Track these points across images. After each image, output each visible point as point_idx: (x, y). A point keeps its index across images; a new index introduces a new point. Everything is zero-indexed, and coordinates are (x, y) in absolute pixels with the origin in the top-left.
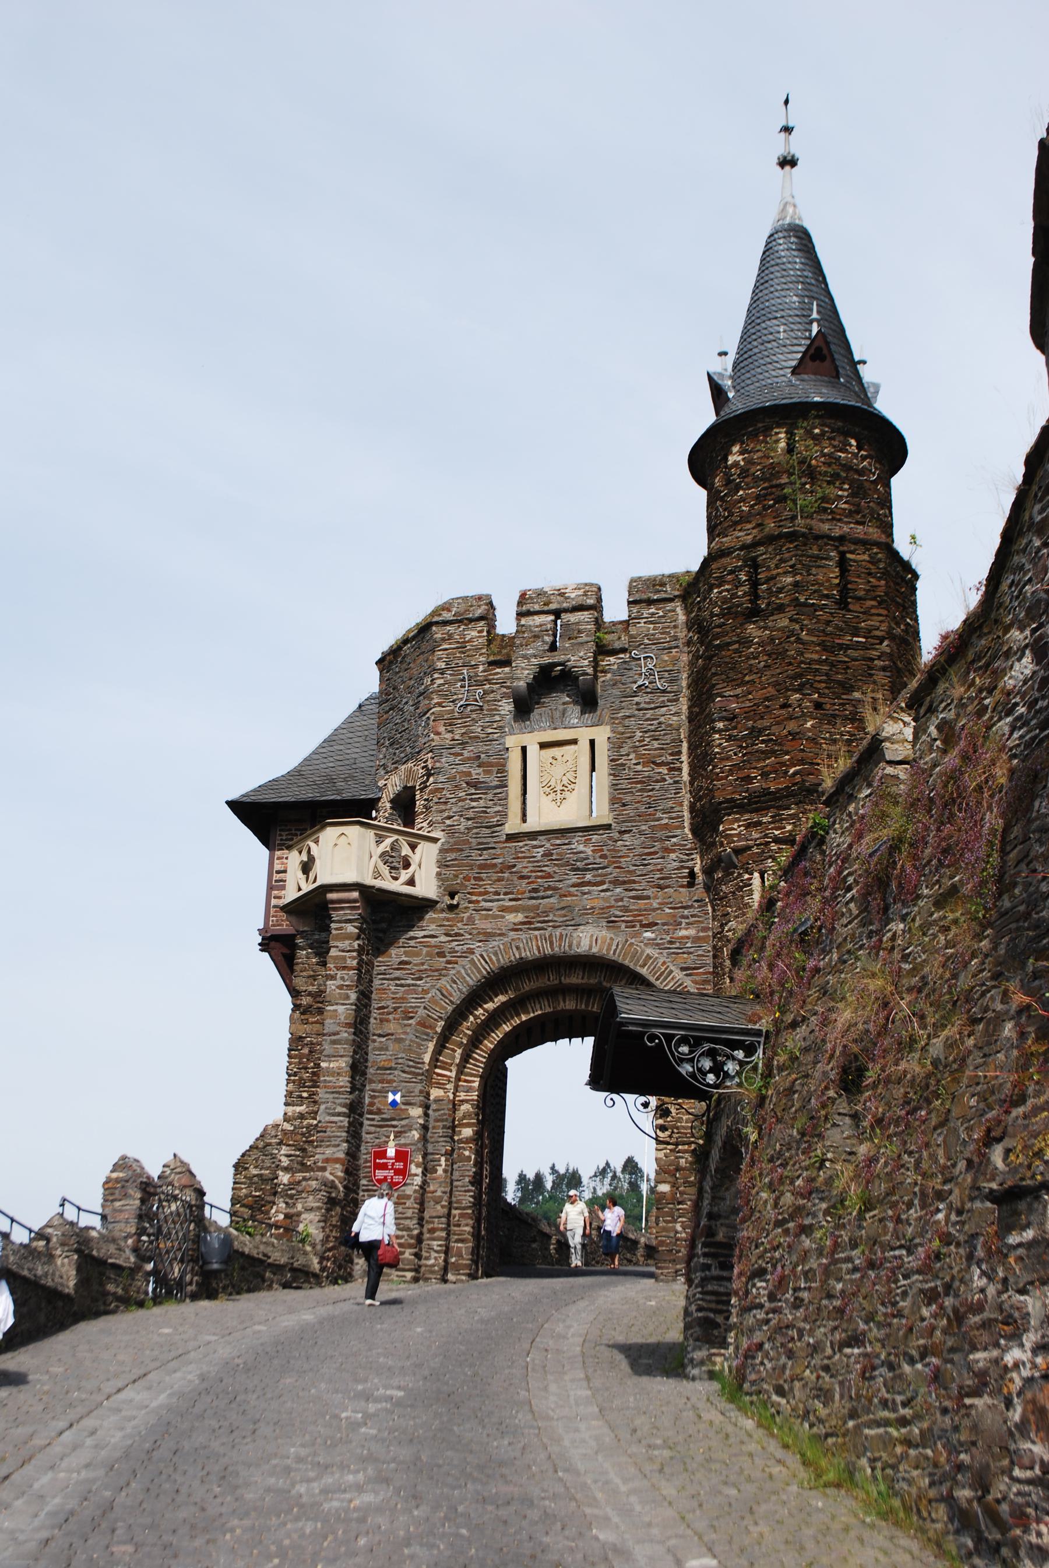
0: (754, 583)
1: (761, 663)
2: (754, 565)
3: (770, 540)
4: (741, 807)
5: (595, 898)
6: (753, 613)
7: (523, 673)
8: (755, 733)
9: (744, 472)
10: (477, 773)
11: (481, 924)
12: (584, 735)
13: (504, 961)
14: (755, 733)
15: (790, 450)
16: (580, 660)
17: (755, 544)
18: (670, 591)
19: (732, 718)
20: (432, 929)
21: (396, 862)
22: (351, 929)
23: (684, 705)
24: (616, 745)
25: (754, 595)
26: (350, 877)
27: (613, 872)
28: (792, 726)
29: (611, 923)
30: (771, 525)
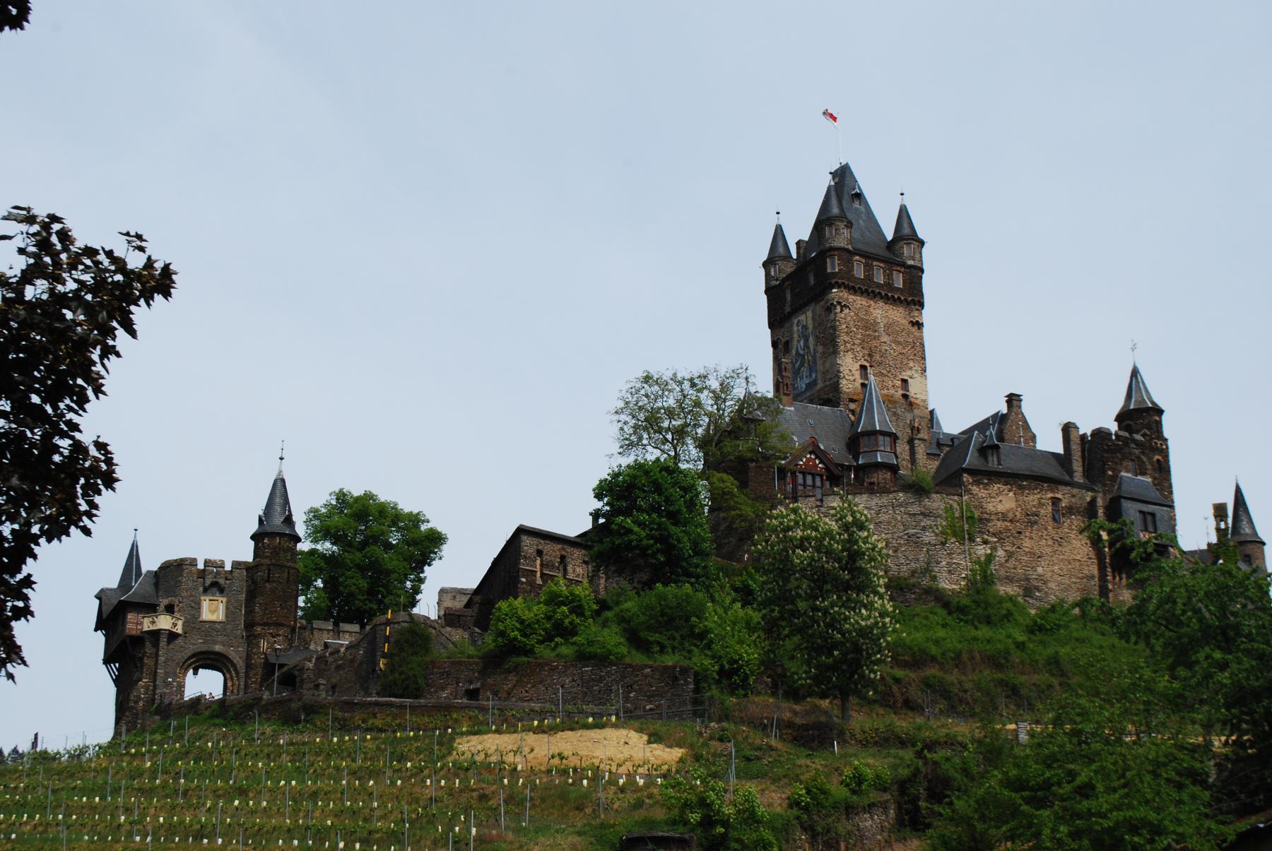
0: (269, 574)
1: (269, 593)
2: (269, 570)
3: (274, 565)
4: (261, 625)
5: (220, 638)
6: (268, 581)
7: (208, 582)
8: (266, 609)
9: (268, 546)
10: (193, 605)
11: (192, 641)
12: (220, 599)
13: (198, 650)
14: (266, 609)
15: (280, 543)
16: (222, 581)
17: (270, 565)
18: (243, 566)
19: (260, 604)
20: (180, 641)
21: (175, 625)
22: (165, 640)
23: (244, 596)
24: (227, 603)
25: (269, 577)
26: (167, 628)
27: (225, 633)
28: (274, 609)
29: (224, 645)
30: (274, 561)
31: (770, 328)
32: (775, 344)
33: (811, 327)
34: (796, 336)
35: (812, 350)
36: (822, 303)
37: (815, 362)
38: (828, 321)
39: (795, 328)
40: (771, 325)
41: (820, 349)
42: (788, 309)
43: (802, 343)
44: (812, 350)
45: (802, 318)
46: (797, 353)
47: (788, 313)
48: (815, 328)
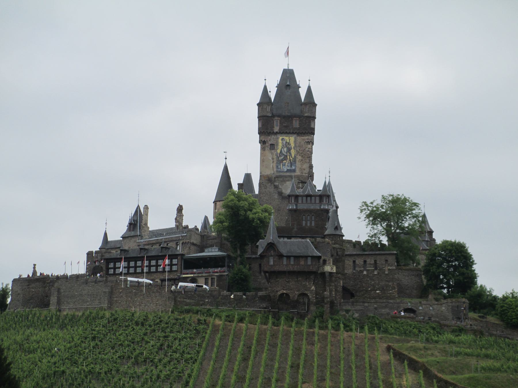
31: (259, 133)
32: (263, 142)
33: (293, 145)
34: (280, 145)
35: (293, 156)
36: (303, 138)
37: (295, 161)
38: (307, 147)
39: (280, 141)
40: (260, 133)
41: (299, 158)
42: (276, 129)
43: (285, 149)
44: (293, 156)
45: (286, 138)
46: (281, 151)
47: (277, 132)
48: (295, 146)
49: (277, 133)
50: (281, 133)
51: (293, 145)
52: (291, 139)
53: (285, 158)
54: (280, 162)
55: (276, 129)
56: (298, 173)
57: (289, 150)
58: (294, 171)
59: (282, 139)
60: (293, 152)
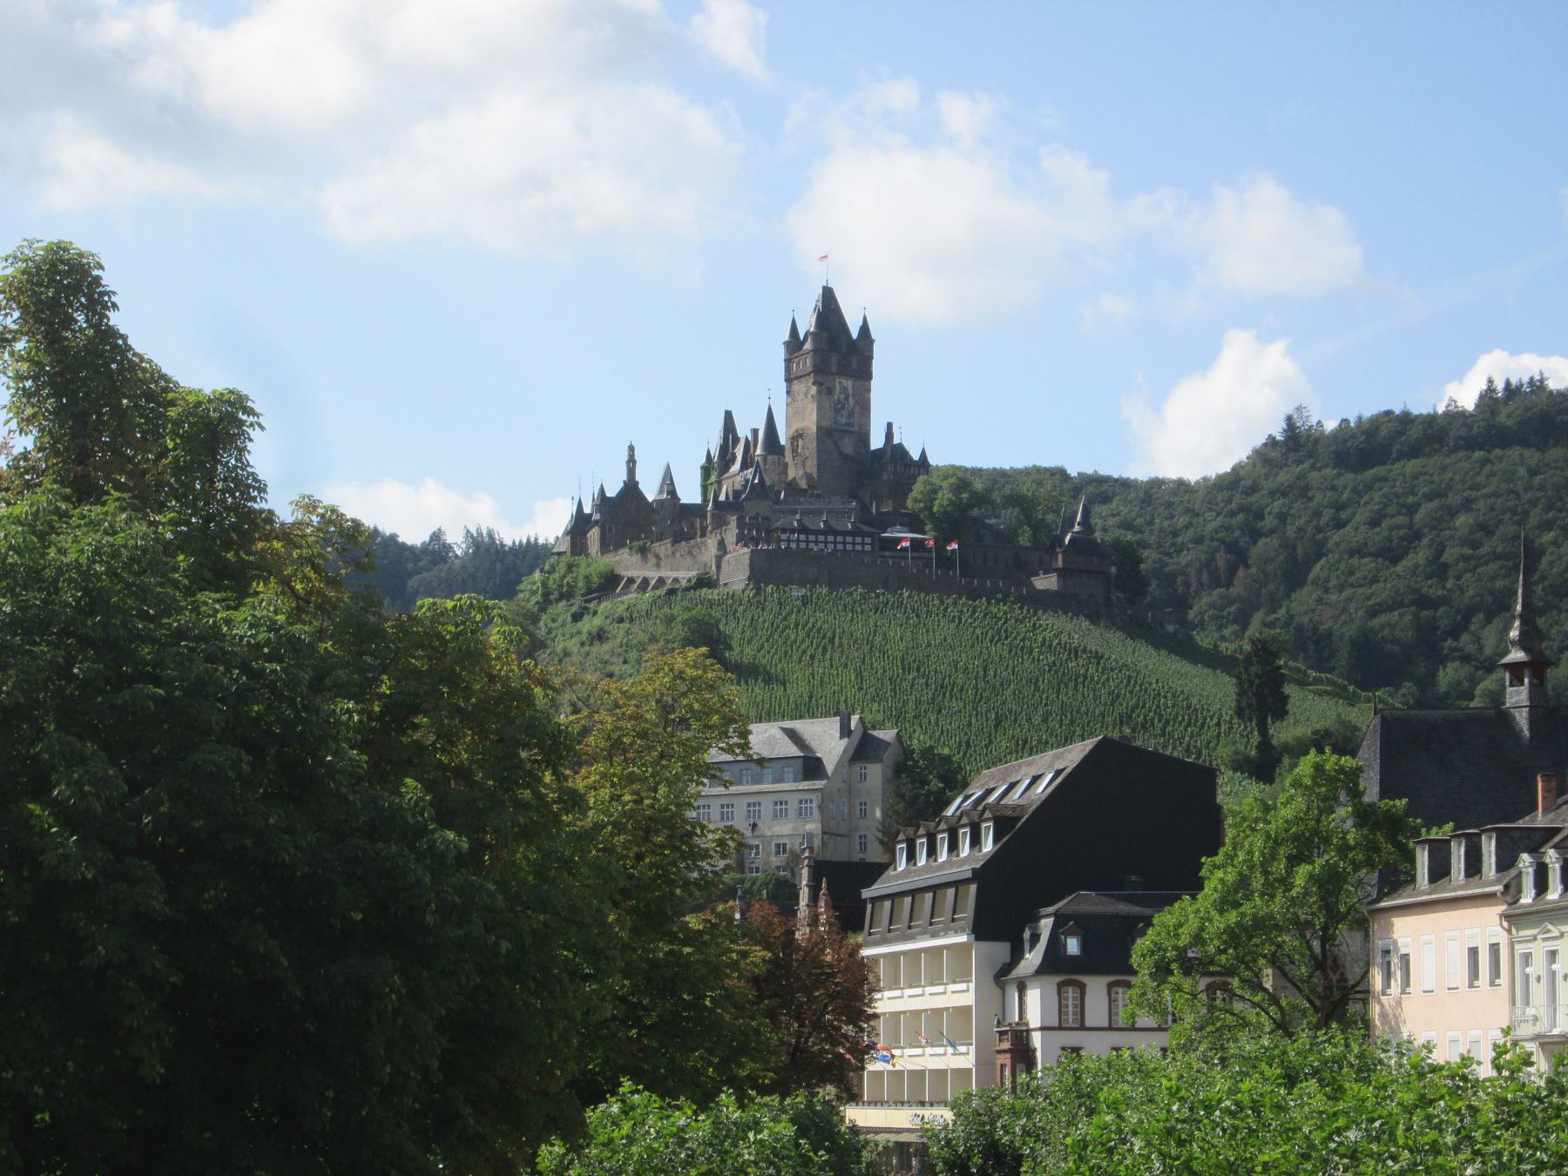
33: (850, 391)
37: (853, 413)
41: (857, 409)
42: (834, 370)
45: (844, 381)
49: (833, 374)
50: (840, 374)
51: (850, 391)
52: (848, 383)
53: (843, 408)
54: (838, 411)
55: (834, 370)
56: (856, 428)
57: (847, 397)
58: (852, 425)
59: (840, 383)
60: (851, 399)
